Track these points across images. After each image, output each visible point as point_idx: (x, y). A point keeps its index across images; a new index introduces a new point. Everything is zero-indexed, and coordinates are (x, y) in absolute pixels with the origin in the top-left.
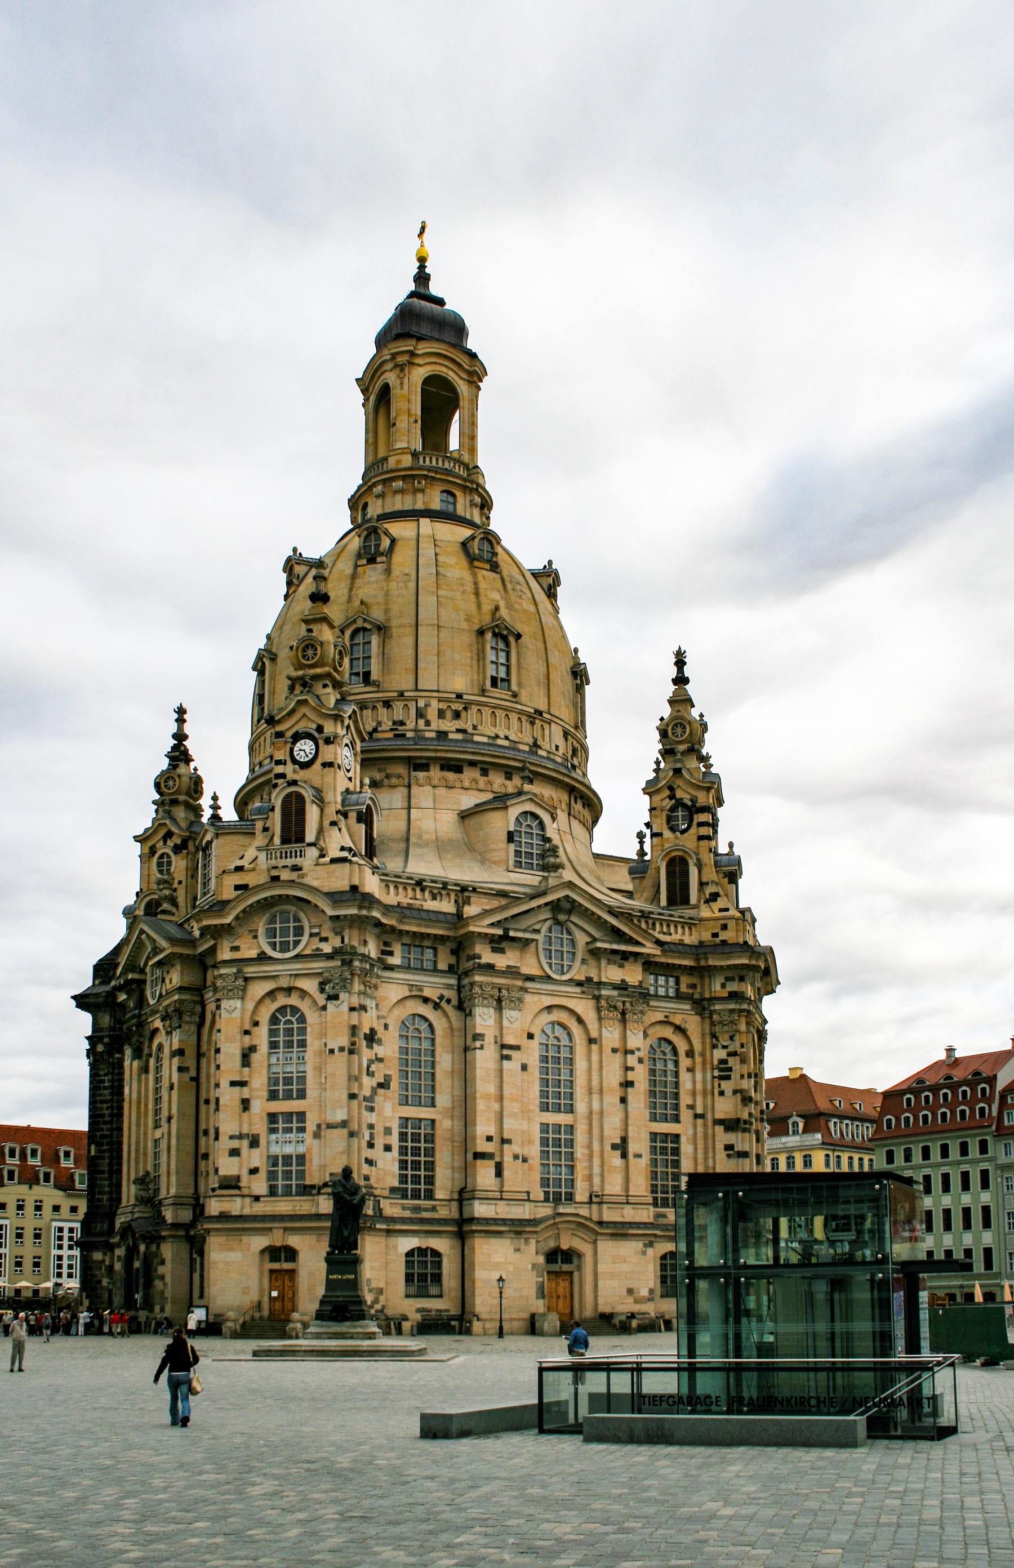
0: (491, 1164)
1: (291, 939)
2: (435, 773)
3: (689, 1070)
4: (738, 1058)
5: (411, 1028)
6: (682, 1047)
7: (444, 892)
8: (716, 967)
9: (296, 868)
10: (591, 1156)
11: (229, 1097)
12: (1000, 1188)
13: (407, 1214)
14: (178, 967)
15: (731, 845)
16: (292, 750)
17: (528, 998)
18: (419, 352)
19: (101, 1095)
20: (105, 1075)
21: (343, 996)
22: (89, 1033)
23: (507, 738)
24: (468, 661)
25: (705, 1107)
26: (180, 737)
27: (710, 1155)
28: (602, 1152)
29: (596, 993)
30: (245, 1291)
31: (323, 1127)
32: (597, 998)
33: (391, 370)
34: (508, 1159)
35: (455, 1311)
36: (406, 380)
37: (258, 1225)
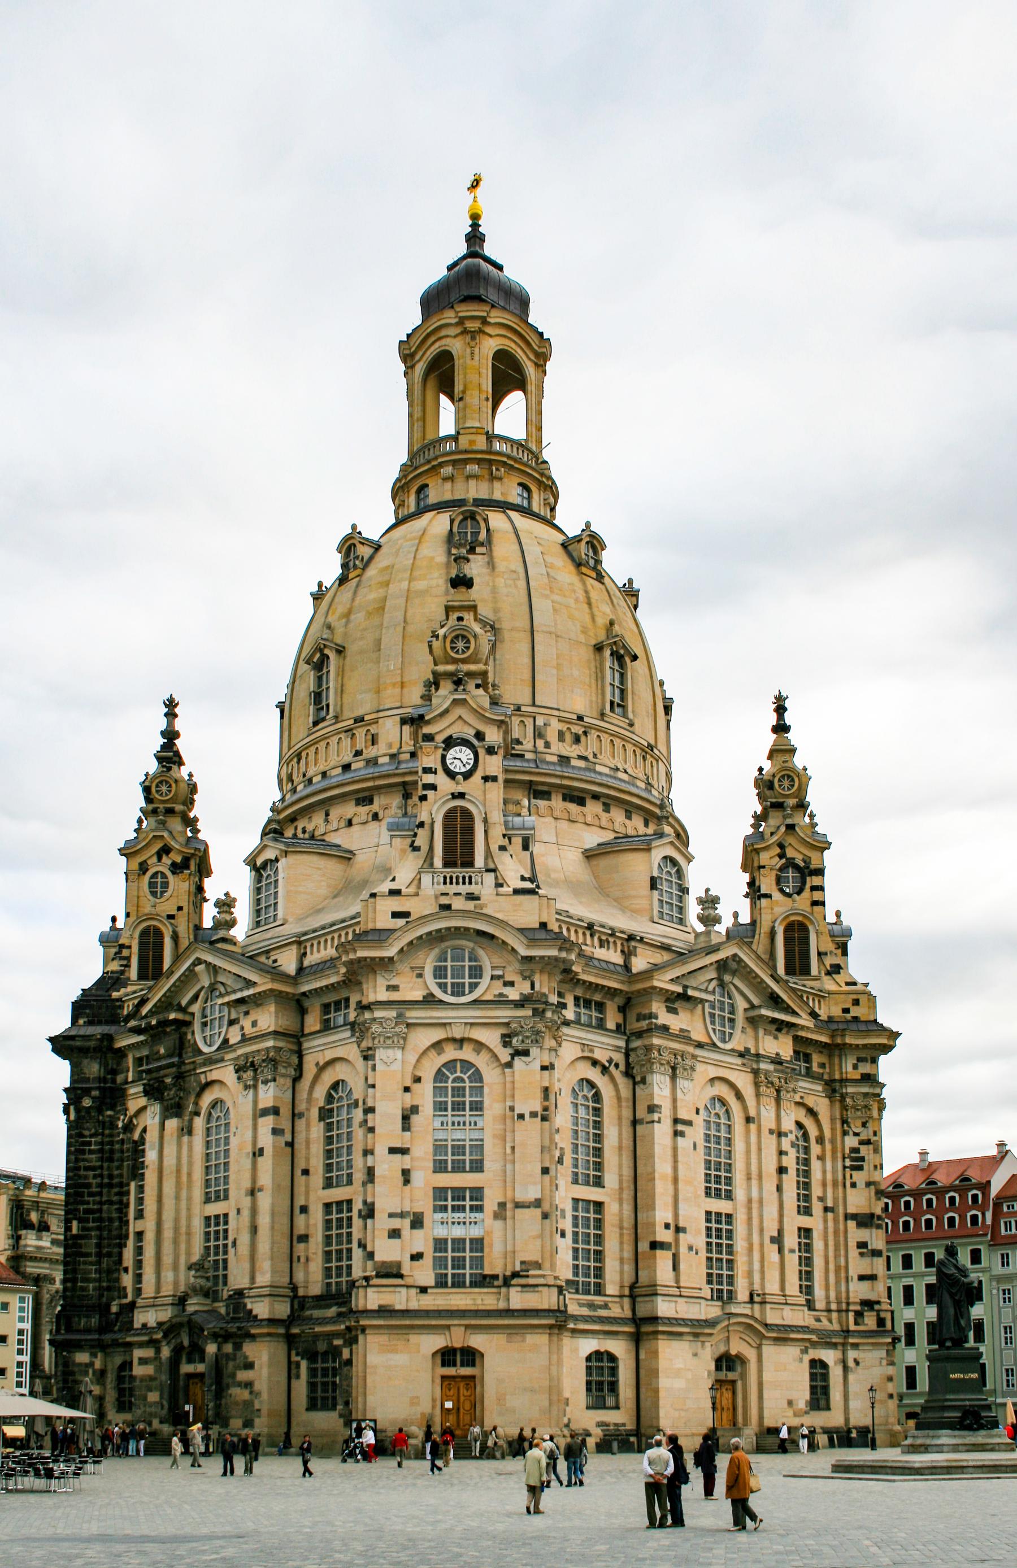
0: (669, 1254)
1: (467, 980)
2: (557, 802)
3: (819, 1158)
4: (871, 1147)
5: (581, 1094)
6: (813, 1132)
7: (611, 940)
8: (851, 1045)
9: (471, 897)
10: (750, 1249)
11: (387, 1166)
12: (995, 1302)
13: (585, 1311)
14: (272, 1008)
15: (838, 914)
16: (444, 758)
17: (700, 1067)
18: (492, 321)
19: (84, 1160)
20: (91, 1136)
21: (534, 1051)
22: (68, 1085)
23: (626, 772)
24: (587, 680)
25: (835, 1199)
26: (170, 736)
27: (842, 1252)
28: (762, 1245)
29: (755, 1066)
30: (414, 1401)
31: (509, 1206)
32: (756, 1072)
33: (455, 337)
34: (683, 1250)
35: (631, 1426)
36: (477, 350)
37: (434, 1322)
